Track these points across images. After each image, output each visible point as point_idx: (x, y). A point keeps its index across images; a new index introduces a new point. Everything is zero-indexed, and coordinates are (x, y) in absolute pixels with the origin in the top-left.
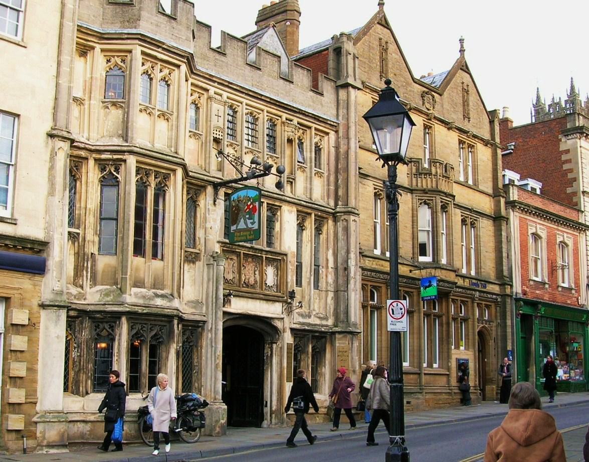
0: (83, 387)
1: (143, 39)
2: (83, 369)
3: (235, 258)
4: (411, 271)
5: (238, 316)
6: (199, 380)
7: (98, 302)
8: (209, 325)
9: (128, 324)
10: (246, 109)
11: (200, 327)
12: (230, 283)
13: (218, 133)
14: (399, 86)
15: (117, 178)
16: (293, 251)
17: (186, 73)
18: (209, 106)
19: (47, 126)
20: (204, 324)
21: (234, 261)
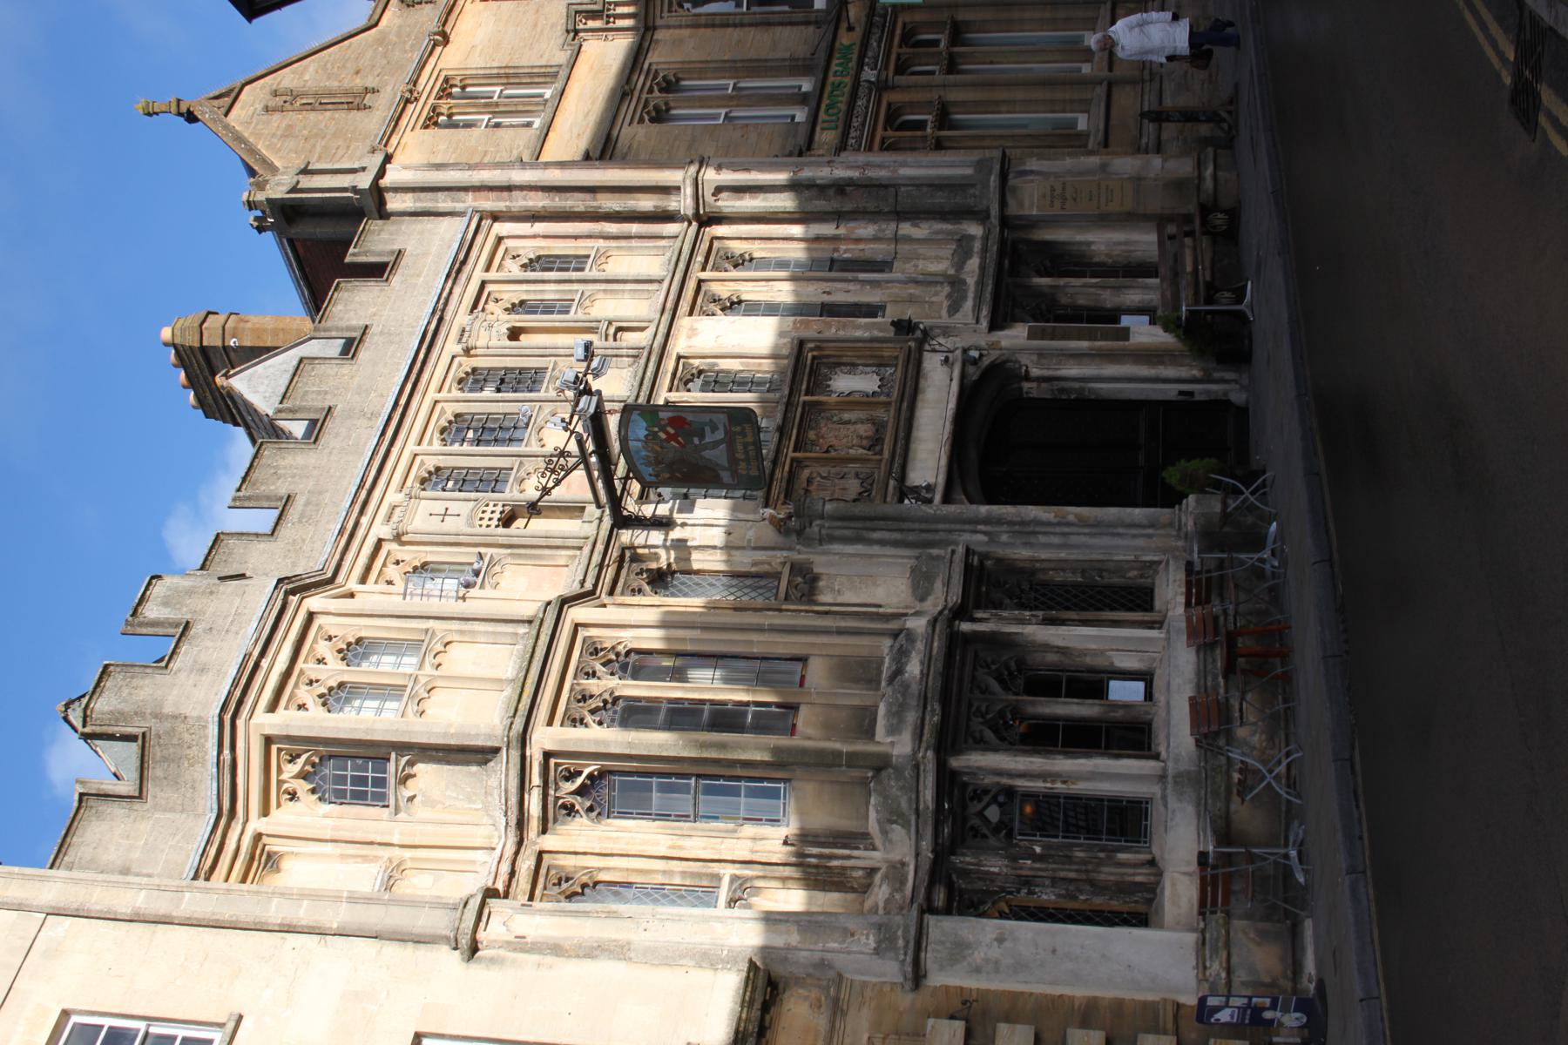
0: (1134, 875)
1: (232, 709)
2: (1087, 871)
3: (806, 473)
4: (850, 29)
5: (955, 466)
6: (1120, 569)
7: (909, 831)
8: (978, 540)
9: (975, 749)
10: (430, 443)
11: (981, 562)
12: (871, 485)
13: (487, 516)
14: (385, 62)
15: (590, 776)
16: (791, 324)
17: (326, 597)
18: (419, 538)
19: (448, 959)
20: (974, 553)
21: (815, 475)
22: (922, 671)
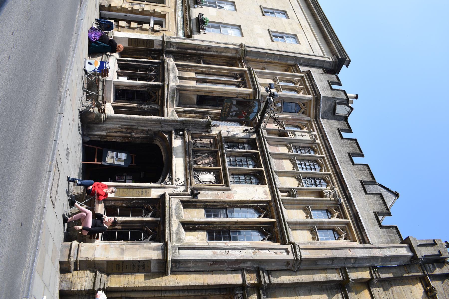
22: (170, 75)
